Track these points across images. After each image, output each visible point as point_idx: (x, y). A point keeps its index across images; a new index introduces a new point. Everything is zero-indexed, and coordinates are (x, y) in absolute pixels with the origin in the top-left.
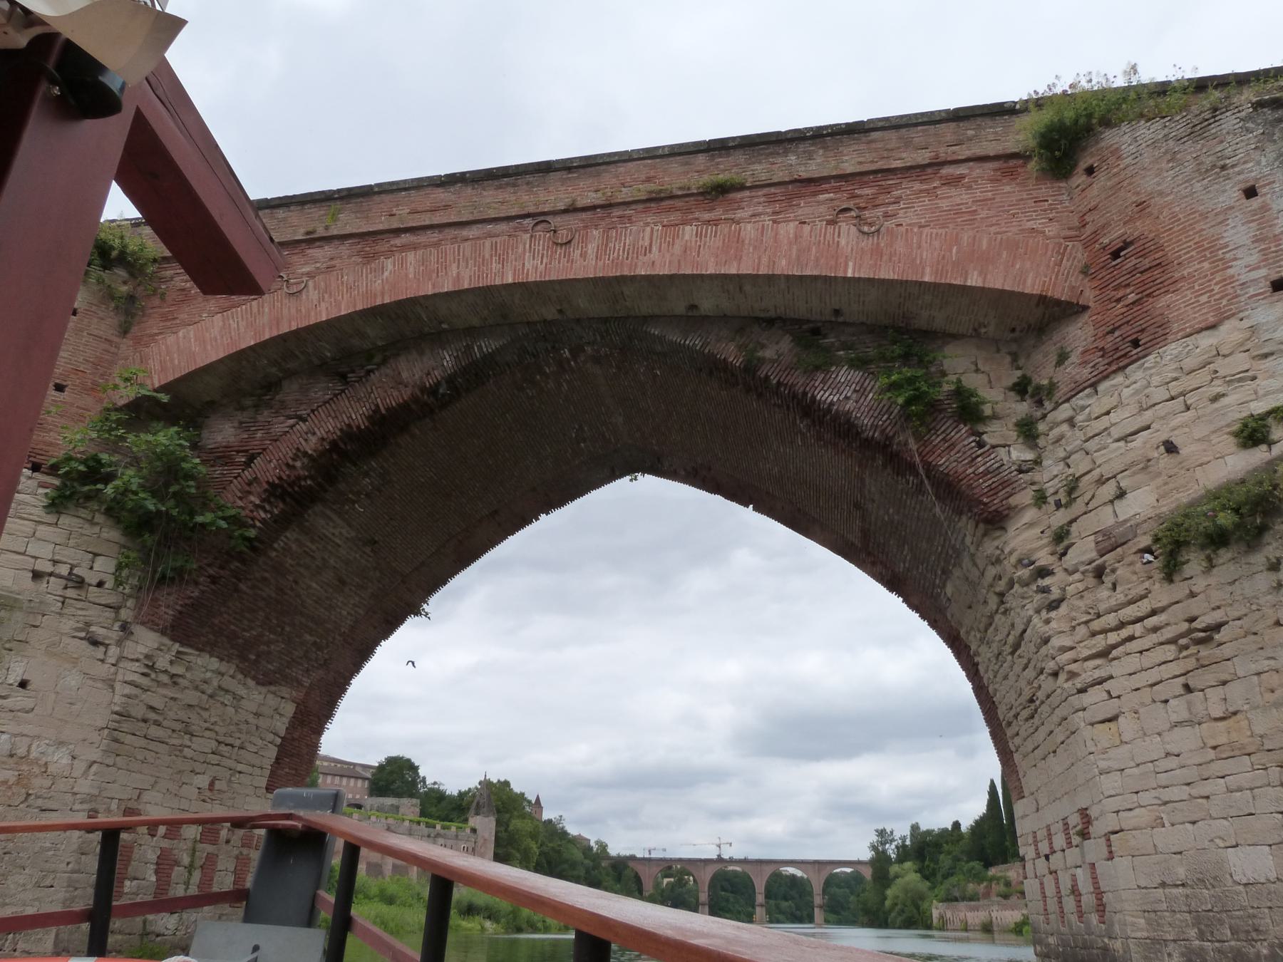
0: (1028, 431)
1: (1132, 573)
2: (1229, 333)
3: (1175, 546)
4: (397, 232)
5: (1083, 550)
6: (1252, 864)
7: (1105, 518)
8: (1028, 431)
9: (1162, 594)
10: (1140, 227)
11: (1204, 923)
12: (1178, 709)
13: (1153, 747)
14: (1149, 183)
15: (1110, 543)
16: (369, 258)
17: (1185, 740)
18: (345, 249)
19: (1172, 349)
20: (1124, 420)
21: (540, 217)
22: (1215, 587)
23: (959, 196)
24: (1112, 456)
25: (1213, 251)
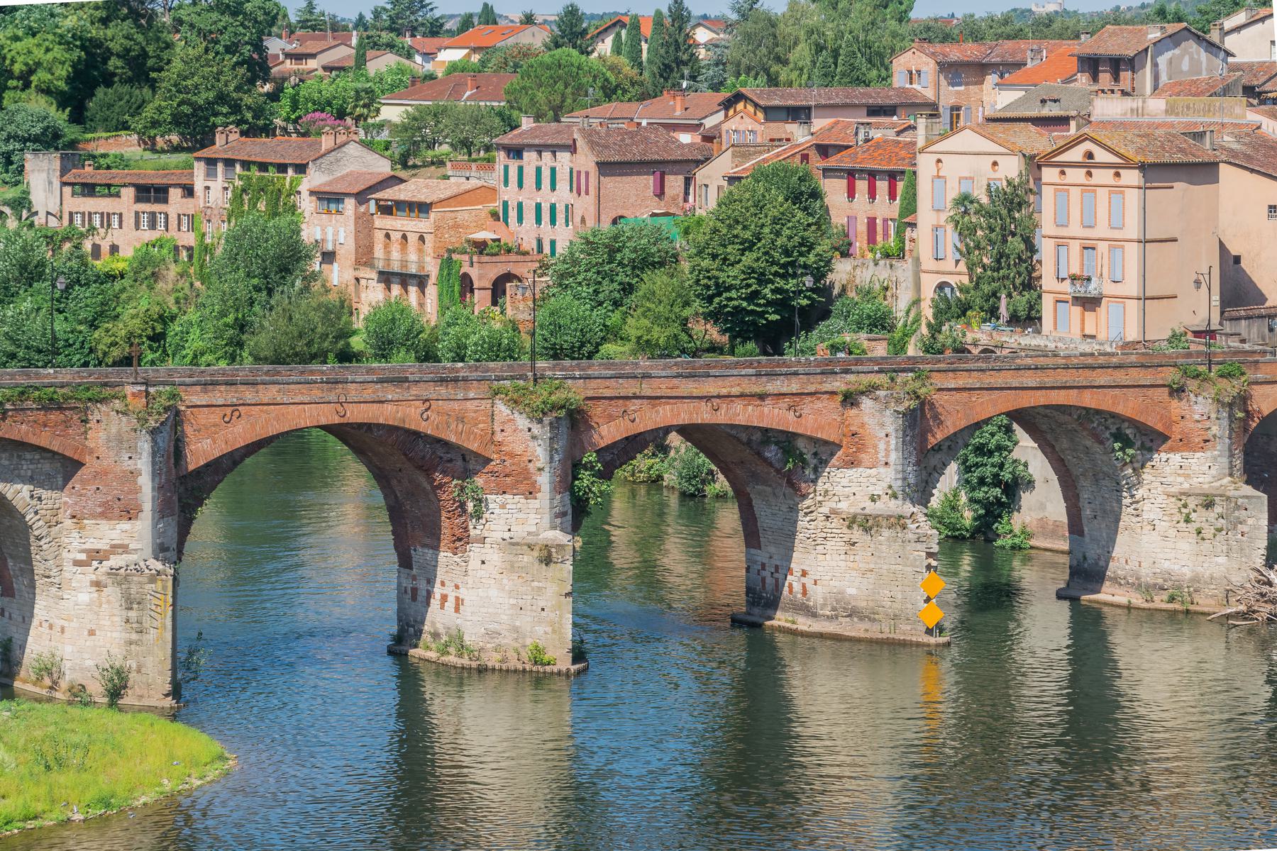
0: (815, 470)
1: (836, 522)
2: (874, 471)
3: (852, 521)
4: (661, 397)
5: (825, 510)
6: (851, 591)
7: (834, 505)
8: (815, 470)
9: (845, 530)
10: (861, 431)
11: (838, 601)
12: (843, 557)
13: (834, 564)
14: (866, 419)
15: (834, 512)
16: (654, 406)
17: (842, 564)
18: (645, 401)
19: (860, 469)
20: (844, 482)
21: (708, 398)
22: (857, 534)
23: (819, 405)
24: (838, 490)
25: (875, 447)
